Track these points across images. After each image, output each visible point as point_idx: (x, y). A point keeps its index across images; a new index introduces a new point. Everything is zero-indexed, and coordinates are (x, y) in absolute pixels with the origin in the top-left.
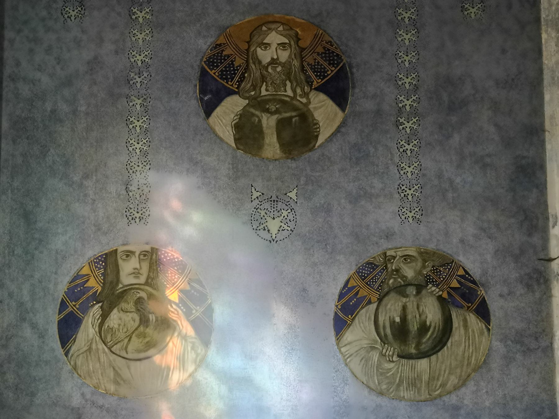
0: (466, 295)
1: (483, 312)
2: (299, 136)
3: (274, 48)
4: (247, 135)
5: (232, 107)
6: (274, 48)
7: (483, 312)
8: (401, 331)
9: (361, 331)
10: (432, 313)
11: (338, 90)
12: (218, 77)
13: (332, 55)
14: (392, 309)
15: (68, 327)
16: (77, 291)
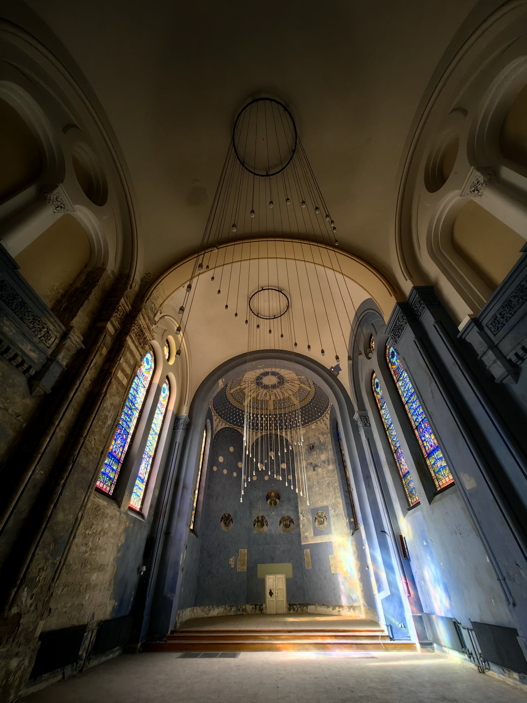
0: (292, 521)
1: (293, 523)
2: (275, 504)
3: (273, 494)
4: (271, 503)
5: (269, 500)
6: (273, 494)
7: (293, 523)
8: (286, 525)
9: (282, 525)
10: (289, 523)
11: (279, 500)
12: (268, 497)
13: (278, 495)
14: (285, 523)
15: (254, 525)
16: (255, 521)
